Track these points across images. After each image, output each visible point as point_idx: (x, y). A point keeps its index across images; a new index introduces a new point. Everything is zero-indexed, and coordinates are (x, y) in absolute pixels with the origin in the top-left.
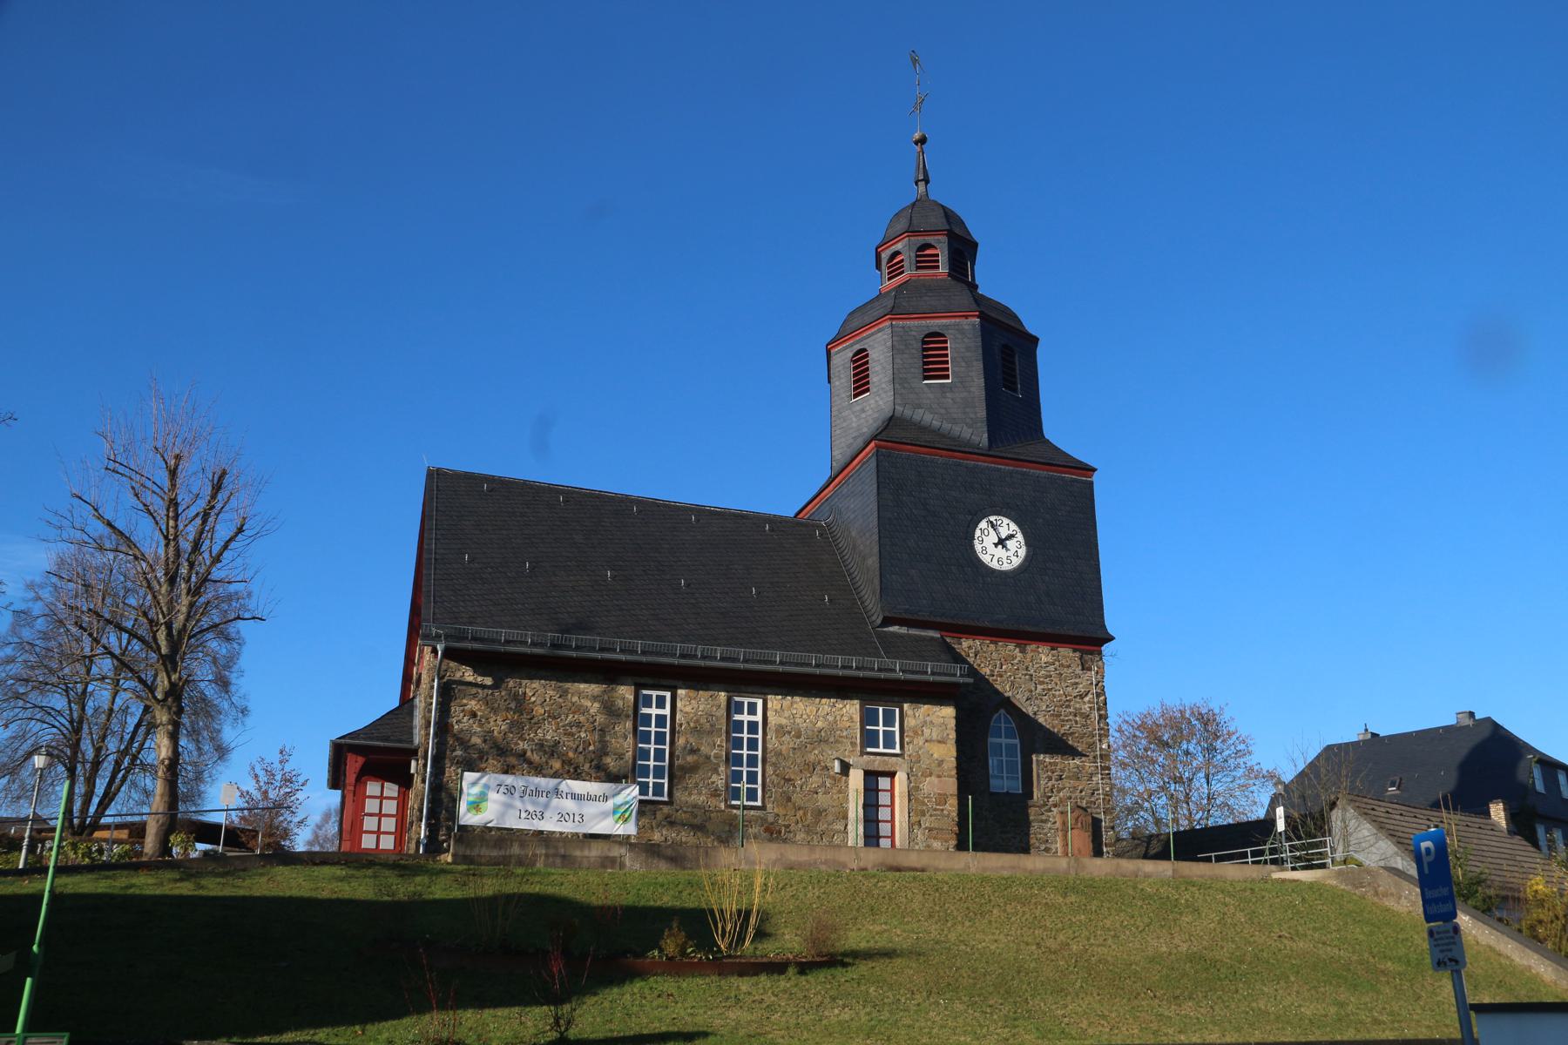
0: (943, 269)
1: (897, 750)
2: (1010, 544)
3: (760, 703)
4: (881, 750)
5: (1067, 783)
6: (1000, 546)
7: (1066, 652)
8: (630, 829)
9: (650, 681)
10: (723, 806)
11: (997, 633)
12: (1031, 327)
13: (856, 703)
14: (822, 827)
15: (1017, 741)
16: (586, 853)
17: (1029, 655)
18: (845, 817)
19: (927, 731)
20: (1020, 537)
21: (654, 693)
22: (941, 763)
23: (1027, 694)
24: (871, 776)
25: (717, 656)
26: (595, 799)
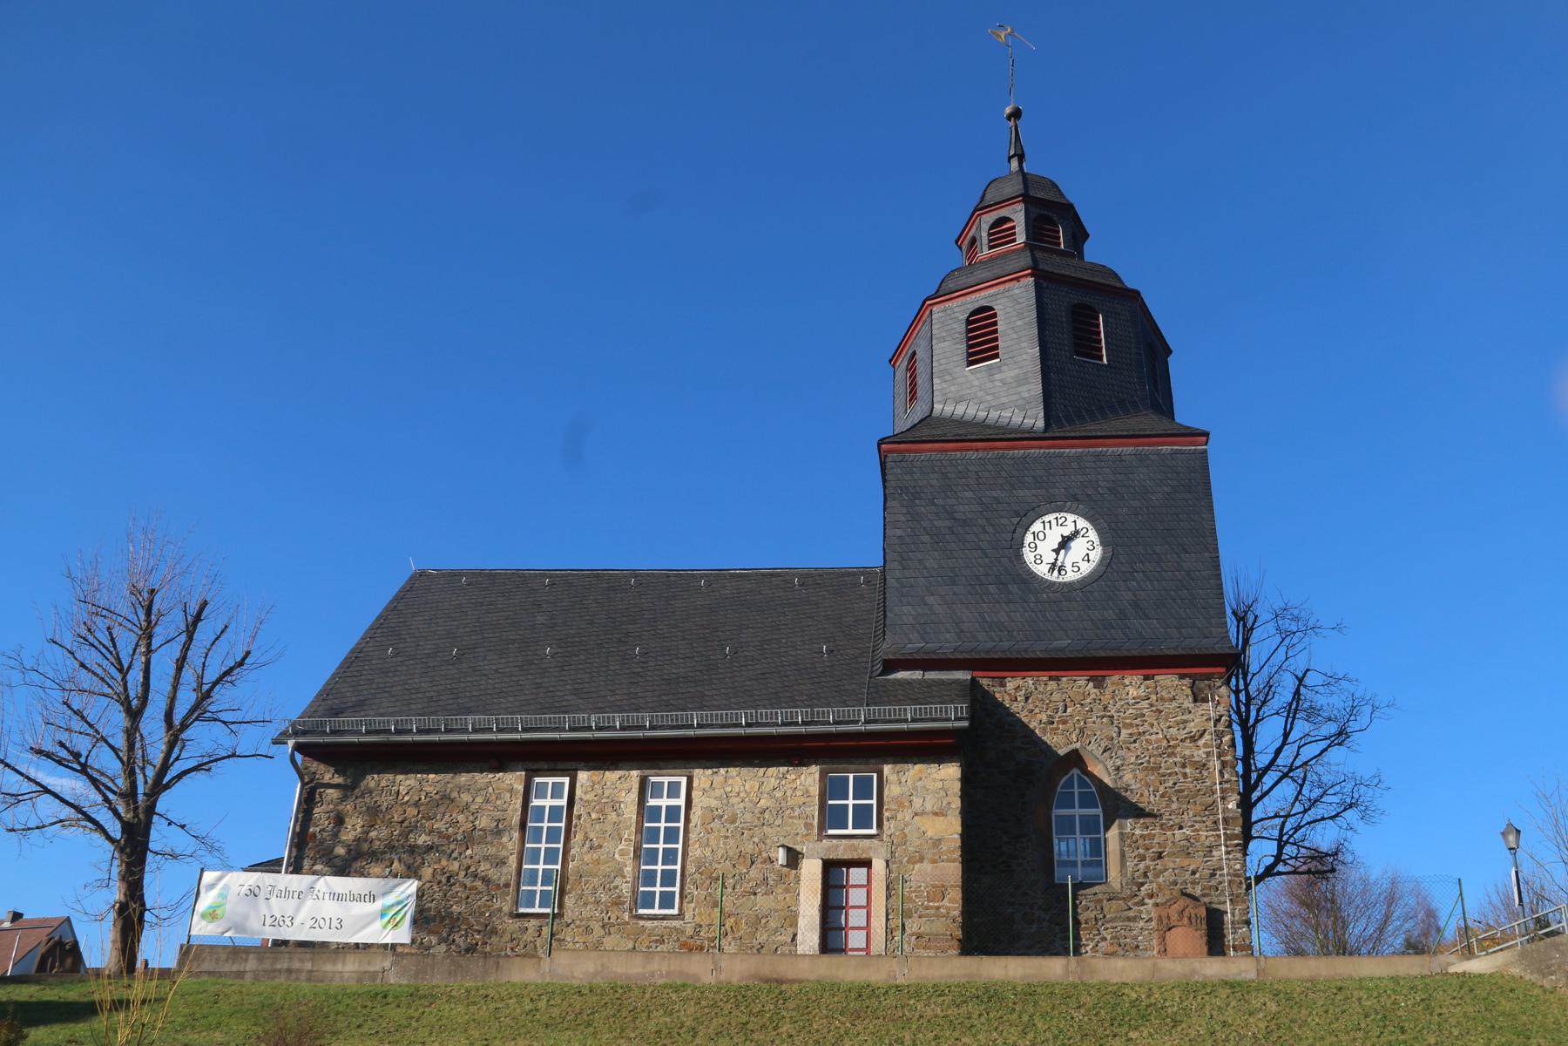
2: (1078, 547)
3: (684, 780)
5: (1168, 862)
6: (1064, 548)
7: (1168, 681)
8: (403, 935)
9: (552, 766)
10: (626, 916)
11: (1056, 665)
12: (1130, 283)
13: (815, 770)
14: (762, 937)
15: (1099, 811)
16: (339, 967)
17: (1109, 690)
18: (794, 924)
19: (918, 802)
20: (1093, 535)
21: (550, 780)
22: (937, 843)
24: (833, 869)
25: (614, 725)
26: (361, 898)
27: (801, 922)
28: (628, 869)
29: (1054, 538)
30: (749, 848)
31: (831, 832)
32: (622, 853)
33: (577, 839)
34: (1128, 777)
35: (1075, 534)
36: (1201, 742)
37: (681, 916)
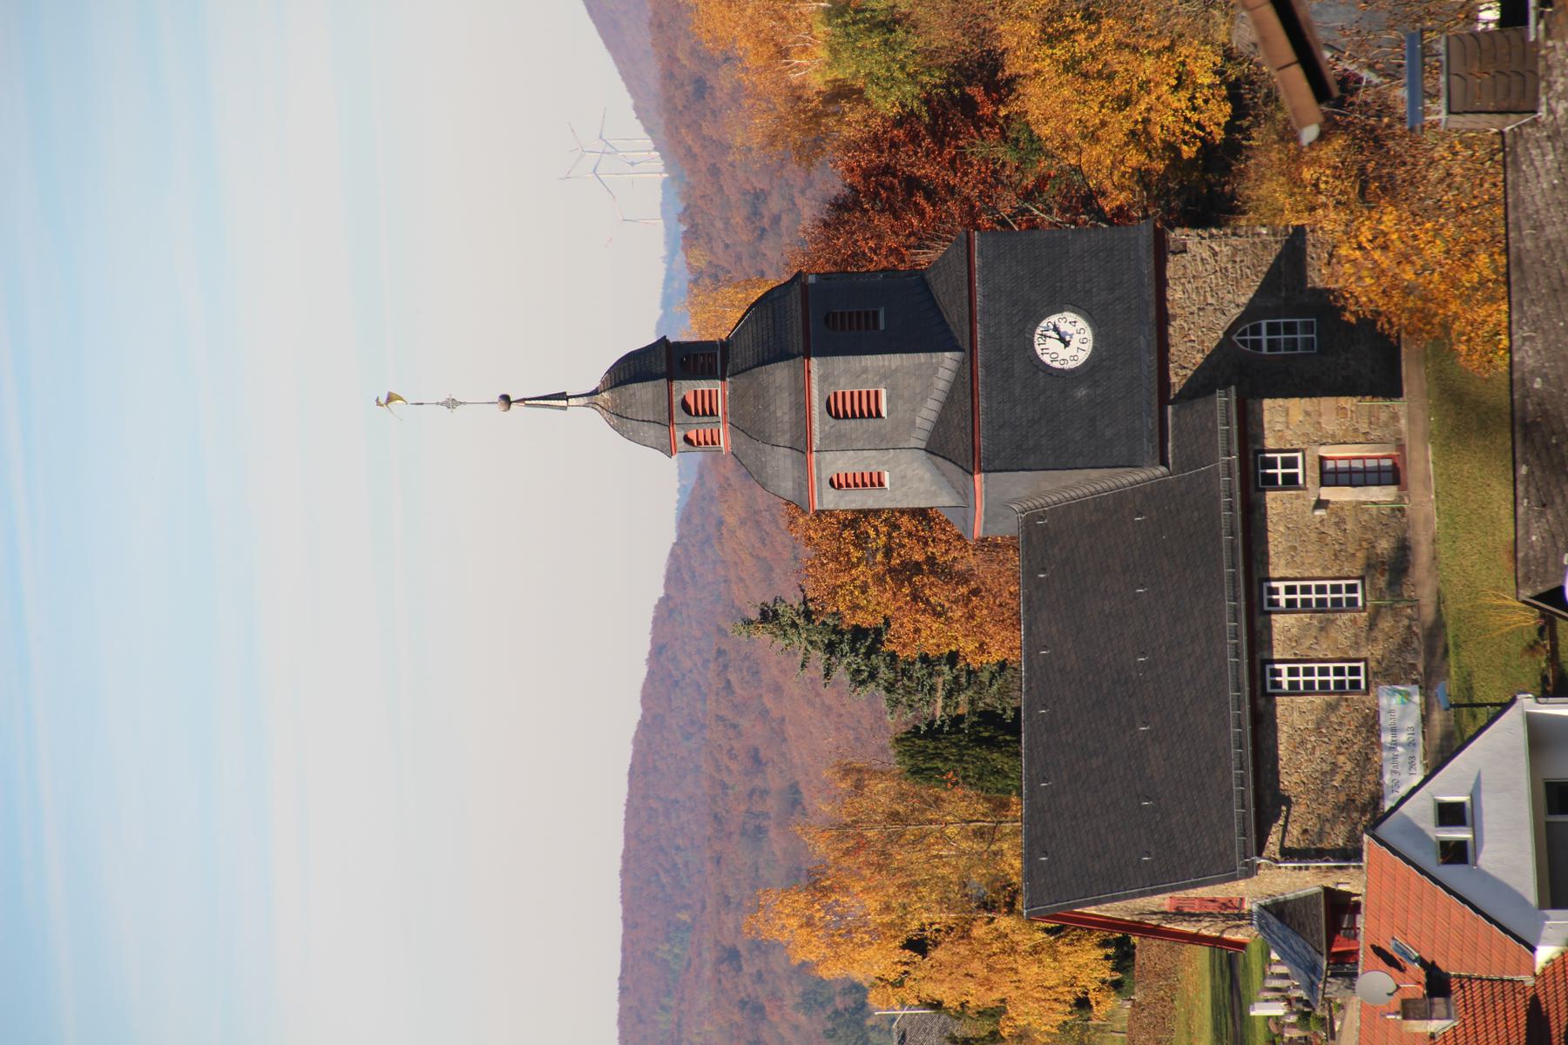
0: (716, 386)
2: (1063, 327)
4: (1299, 471)
7: (1171, 270)
17: (1178, 311)
22: (1307, 413)
23: (1219, 314)
27: (1363, 498)
29: (1054, 345)
30: (1313, 536)
31: (1301, 481)
33: (1313, 655)
35: (1056, 329)
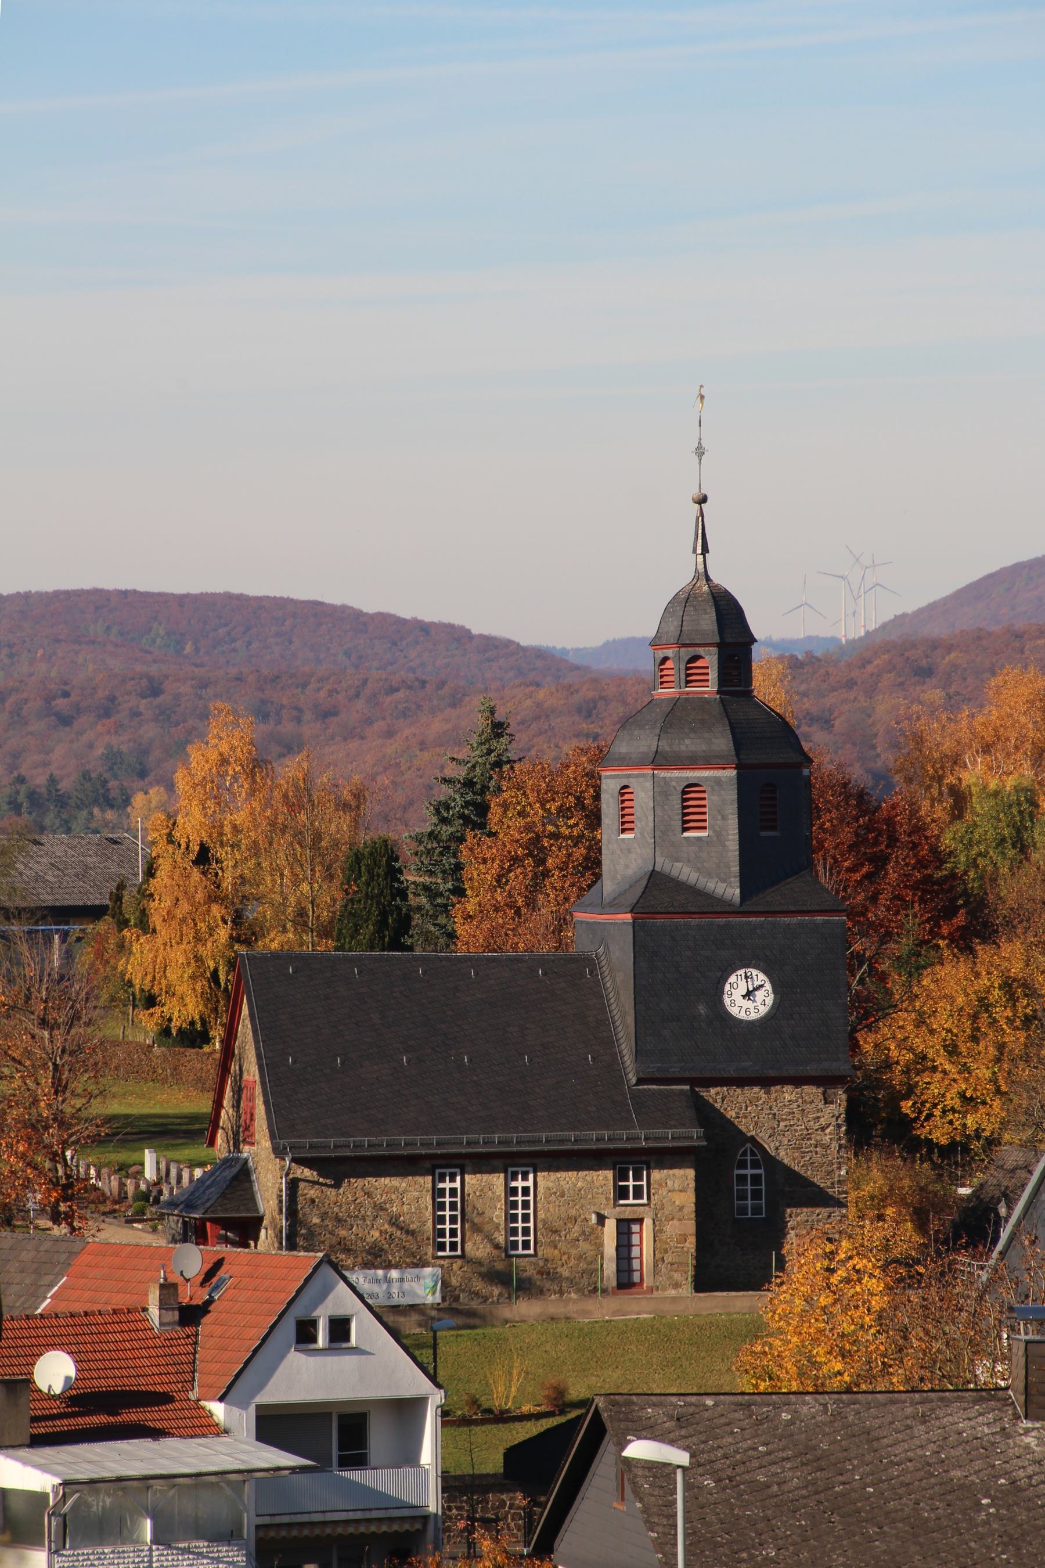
1: (645, 1201)
2: (760, 995)
4: (631, 1201)
10: (503, 1255)
11: (742, 1082)
17: (773, 1096)
20: (768, 986)
22: (681, 1209)
23: (770, 1131)
25: (495, 1140)
28: (502, 1226)
31: (622, 1202)
32: (497, 1217)
34: (782, 1153)
36: (828, 1131)
37: (535, 1255)
